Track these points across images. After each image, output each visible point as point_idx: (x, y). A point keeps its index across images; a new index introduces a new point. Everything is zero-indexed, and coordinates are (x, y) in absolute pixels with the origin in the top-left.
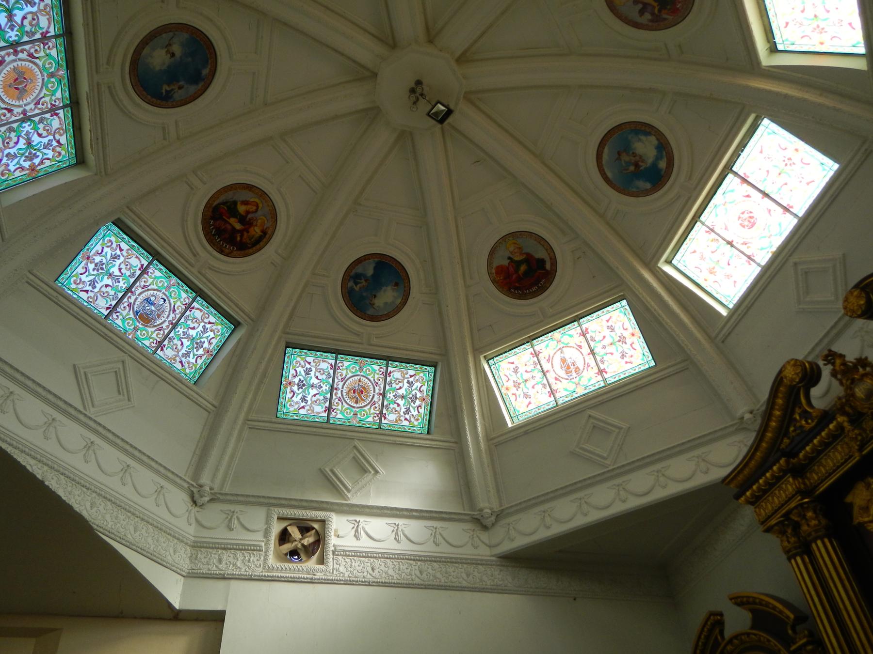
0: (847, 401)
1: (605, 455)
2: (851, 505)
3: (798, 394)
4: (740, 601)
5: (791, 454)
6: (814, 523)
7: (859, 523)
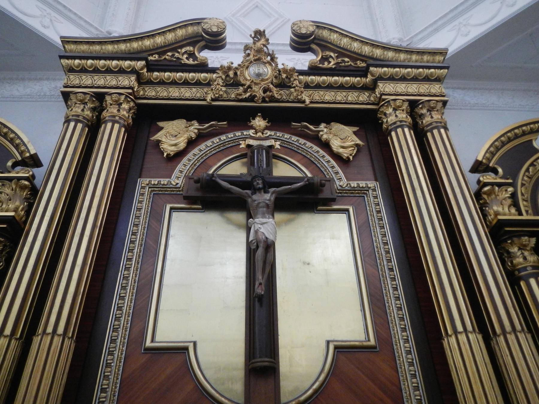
0: (236, 68)
2: (162, 128)
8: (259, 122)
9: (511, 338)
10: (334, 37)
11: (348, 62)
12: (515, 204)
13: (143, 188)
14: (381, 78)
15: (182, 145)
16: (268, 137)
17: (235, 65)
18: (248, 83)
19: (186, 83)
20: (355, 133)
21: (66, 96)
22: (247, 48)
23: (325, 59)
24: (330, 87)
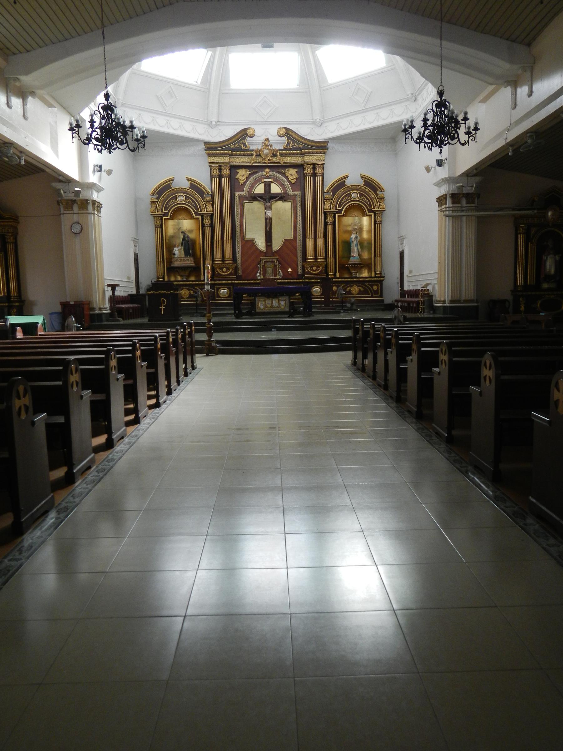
1: (167, 105)
2: (238, 172)
3: (246, 136)
4: (188, 179)
5: (232, 151)
6: (228, 172)
7: (238, 179)
8: (267, 170)
9: (319, 239)
10: (293, 134)
11: (296, 145)
12: (330, 206)
13: (237, 196)
14: (305, 153)
15: (245, 181)
16: (270, 175)
17: (259, 149)
19: (244, 155)
20: (296, 172)
21: (210, 166)
22: (262, 143)
23: (288, 144)
24: (290, 154)
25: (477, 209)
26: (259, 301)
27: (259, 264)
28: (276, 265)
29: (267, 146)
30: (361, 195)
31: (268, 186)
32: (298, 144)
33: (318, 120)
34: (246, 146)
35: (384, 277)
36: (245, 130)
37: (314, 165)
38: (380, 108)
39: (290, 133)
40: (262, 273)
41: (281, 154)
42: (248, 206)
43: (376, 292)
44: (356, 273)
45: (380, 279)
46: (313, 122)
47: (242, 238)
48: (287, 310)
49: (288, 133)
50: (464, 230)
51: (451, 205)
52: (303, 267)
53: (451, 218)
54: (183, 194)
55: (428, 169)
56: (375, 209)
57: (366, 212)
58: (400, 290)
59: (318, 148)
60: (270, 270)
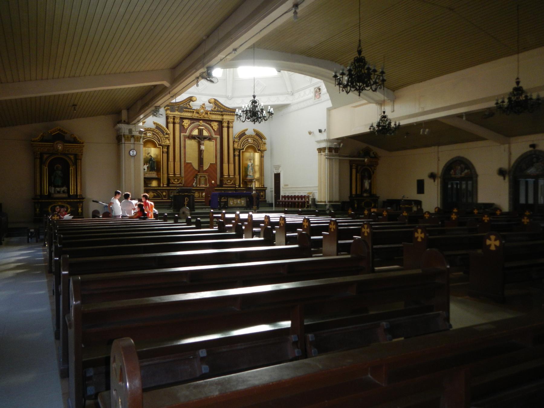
2: (183, 122)
3: (190, 101)
4: (154, 123)
8: (201, 122)
15: (187, 127)
18: (200, 114)
20: (218, 124)
23: (215, 108)
24: (215, 114)
25: (340, 156)
26: (230, 200)
27: (195, 178)
28: (206, 179)
29: (203, 108)
30: (254, 141)
31: (201, 131)
32: (220, 108)
33: (230, 96)
34: (190, 106)
35: (266, 188)
36: (191, 97)
37: (228, 121)
38: (270, 95)
39: (217, 102)
40: (198, 183)
41: (210, 113)
42: (188, 142)
43: (262, 196)
44: (251, 185)
45: (264, 189)
46: (227, 97)
47: (185, 161)
48: (245, 205)
49: (216, 103)
50: (334, 166)
51: (328, 153)
52: (221, 181)
53: (328, 159)
54: (151, 132)
55: (310, 133)
56: (261, 149)
57: (256, 150)
58: (275, 195)
59: (231, 112)
60: (203, 181)
